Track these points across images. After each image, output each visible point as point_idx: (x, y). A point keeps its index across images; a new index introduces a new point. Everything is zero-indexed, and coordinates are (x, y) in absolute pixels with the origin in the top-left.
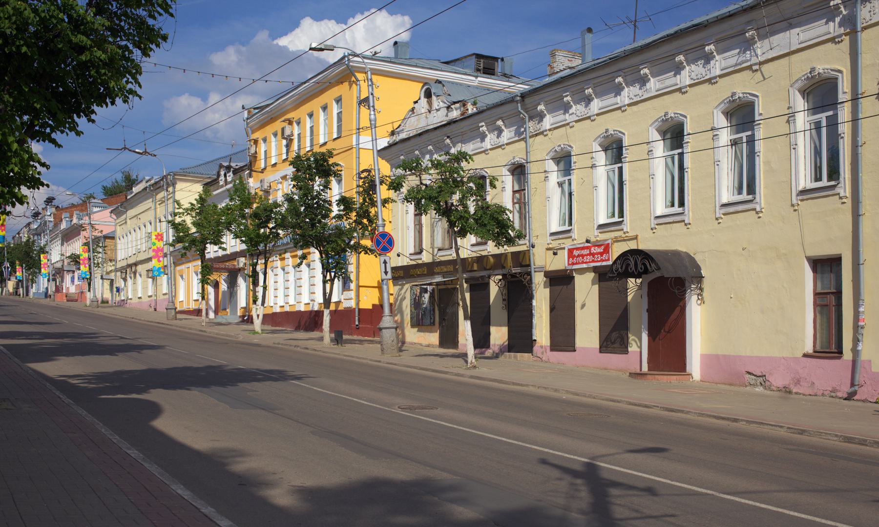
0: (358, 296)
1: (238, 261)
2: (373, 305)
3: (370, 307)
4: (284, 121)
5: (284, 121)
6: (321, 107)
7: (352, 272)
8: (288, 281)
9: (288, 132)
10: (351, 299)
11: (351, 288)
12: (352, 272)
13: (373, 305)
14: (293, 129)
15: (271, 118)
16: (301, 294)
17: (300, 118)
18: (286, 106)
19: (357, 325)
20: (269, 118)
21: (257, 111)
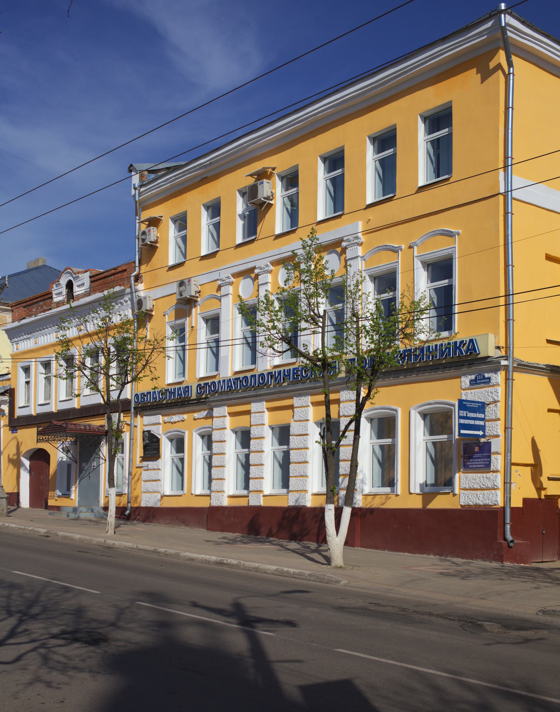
0: (507, 483)
2: (525, 501)
4: (251, 175)
6: (369, 137)
7: (498, 436)
8: (263, 451)
9: (265, 189)
10: (494, 488)
11: (492, 468)
12: (498, 436)
14: (274, 187)
15: (202, 179)
16: (307, 476)
17: (298, 165)
18: (250, 152)
19: (512, 541)
20: (199, 179)
21: (153, 176)
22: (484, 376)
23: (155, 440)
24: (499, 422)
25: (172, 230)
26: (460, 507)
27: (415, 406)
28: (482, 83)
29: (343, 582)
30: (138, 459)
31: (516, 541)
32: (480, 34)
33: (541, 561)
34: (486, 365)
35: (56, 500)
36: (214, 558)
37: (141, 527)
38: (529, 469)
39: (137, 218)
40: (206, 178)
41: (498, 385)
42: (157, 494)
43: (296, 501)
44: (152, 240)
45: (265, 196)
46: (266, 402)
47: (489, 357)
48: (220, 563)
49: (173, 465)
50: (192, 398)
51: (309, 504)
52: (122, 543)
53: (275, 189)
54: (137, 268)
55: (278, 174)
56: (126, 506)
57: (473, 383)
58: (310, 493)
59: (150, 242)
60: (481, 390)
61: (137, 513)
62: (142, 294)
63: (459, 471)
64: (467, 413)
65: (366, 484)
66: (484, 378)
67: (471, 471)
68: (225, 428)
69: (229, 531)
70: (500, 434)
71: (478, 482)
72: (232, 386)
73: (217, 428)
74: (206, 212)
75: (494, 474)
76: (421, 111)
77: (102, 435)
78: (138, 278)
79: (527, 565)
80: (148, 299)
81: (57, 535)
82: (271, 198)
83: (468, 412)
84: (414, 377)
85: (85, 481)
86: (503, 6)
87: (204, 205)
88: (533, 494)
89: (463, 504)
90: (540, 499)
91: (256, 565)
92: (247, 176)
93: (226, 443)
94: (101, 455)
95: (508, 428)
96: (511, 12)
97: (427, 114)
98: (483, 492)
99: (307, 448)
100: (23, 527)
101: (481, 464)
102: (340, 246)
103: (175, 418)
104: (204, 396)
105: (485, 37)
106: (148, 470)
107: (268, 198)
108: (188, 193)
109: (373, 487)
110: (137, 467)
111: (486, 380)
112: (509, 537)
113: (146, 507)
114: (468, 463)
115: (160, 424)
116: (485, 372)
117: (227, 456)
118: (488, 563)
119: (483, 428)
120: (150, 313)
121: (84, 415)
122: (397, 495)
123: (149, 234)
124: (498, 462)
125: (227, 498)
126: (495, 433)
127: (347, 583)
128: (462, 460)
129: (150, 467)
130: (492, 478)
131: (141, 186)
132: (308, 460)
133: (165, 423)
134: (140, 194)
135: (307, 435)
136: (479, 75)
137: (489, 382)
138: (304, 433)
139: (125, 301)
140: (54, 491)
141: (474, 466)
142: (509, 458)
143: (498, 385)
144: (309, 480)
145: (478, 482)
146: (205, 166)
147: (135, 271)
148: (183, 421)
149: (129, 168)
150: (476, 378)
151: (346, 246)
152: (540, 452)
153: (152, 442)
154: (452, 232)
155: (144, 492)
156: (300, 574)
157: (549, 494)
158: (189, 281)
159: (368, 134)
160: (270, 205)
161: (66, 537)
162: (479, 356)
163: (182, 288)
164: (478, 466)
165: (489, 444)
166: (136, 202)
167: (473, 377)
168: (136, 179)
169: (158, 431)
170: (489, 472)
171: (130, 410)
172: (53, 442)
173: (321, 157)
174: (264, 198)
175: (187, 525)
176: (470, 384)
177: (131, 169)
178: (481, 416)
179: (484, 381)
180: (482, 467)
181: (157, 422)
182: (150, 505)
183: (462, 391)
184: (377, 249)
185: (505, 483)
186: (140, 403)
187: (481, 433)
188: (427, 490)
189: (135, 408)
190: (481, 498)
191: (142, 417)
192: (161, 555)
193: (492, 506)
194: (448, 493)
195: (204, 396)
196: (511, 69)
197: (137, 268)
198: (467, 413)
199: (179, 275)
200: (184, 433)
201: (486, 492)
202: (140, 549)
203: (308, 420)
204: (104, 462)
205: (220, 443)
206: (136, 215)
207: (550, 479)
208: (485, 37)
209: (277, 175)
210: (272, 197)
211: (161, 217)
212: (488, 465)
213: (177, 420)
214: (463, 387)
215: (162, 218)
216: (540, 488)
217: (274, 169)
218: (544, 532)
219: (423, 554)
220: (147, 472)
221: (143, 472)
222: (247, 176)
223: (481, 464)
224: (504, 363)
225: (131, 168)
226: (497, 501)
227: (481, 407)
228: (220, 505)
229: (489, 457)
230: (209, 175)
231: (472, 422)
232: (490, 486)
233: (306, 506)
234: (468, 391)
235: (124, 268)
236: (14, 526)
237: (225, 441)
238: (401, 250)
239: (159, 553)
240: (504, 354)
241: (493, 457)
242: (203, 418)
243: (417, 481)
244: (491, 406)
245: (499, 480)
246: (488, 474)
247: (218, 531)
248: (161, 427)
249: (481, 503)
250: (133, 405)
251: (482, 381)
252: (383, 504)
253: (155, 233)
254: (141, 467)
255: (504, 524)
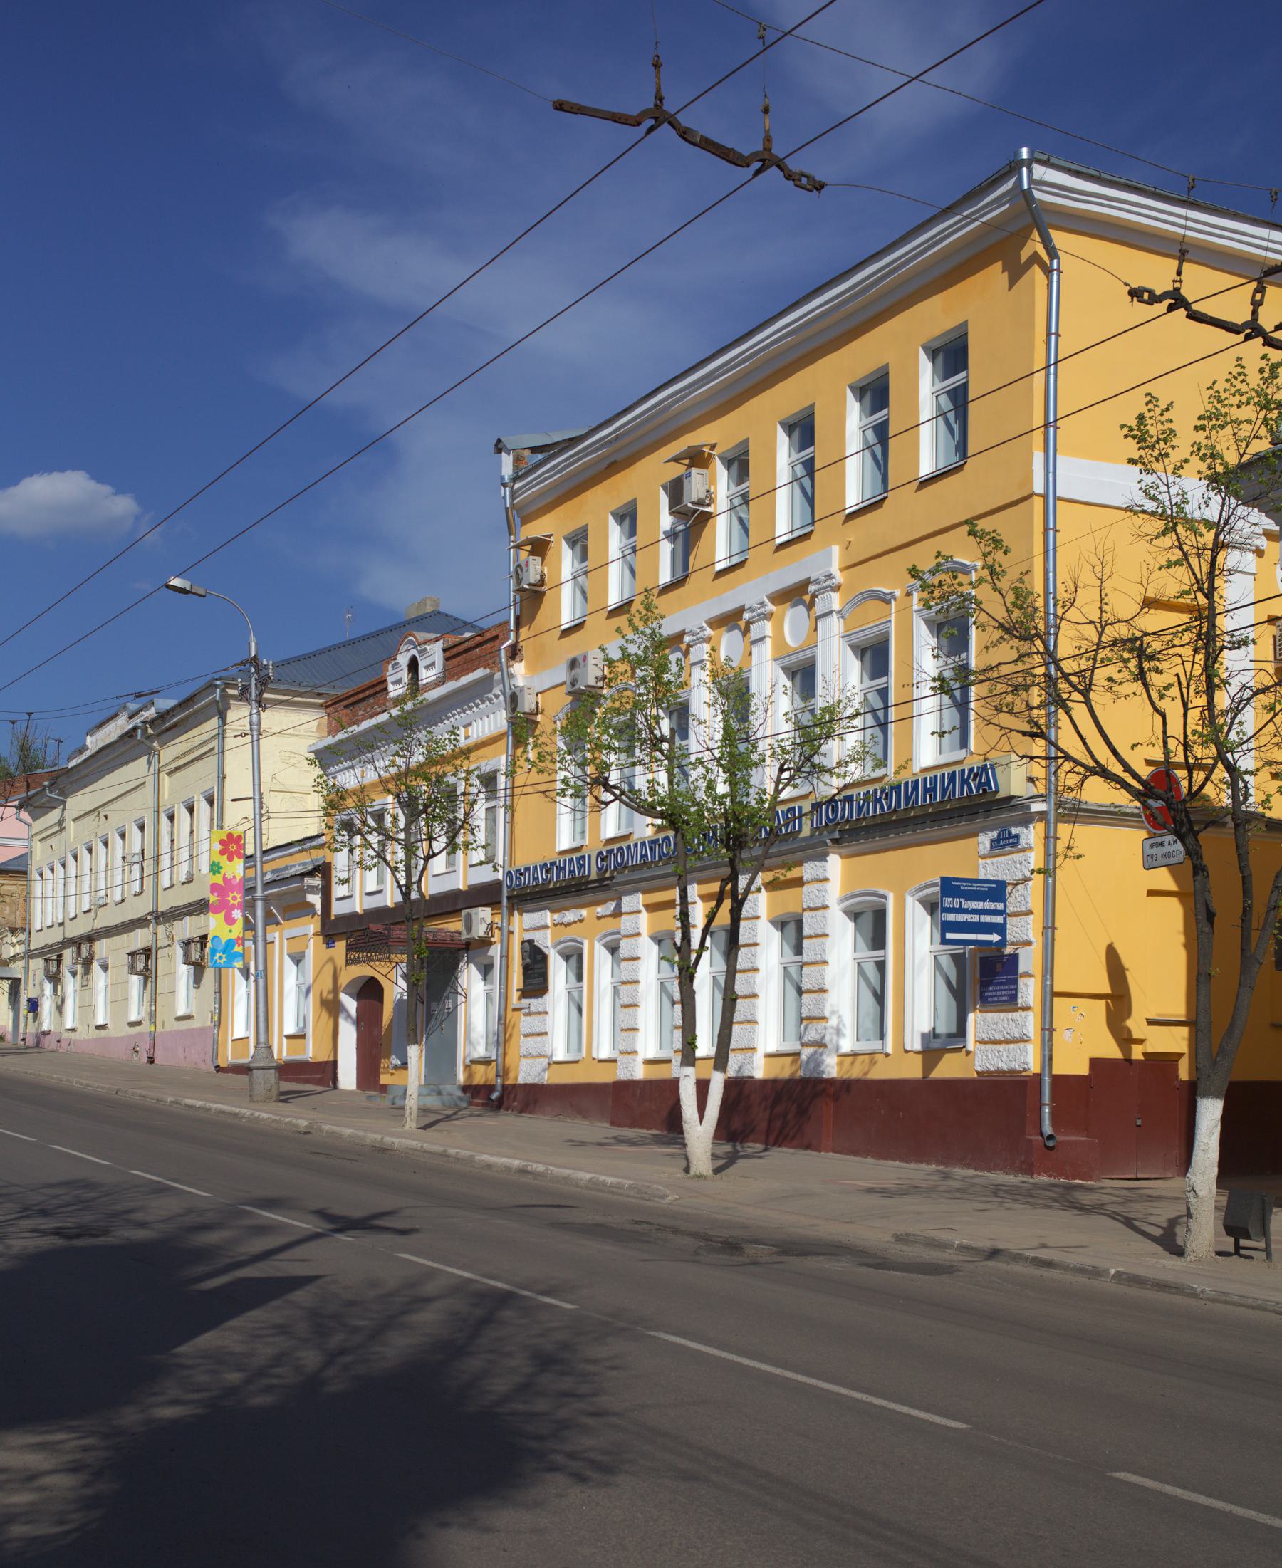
0: (1047, 1029)
1: (469, 917)
2: (1094, 1063)
3: (1084, 1070)
4: (676, 459)
5: (676, 459)
6: (851, 388)
7: (1029, 943)
9: (696, 487)
10: (1024, 1040)
11: (1020, 1002)
12: (1029, 943)
13: (1094, 1063)
14: (713, 480)
16: (755, 1022)
17: (747, 441)
19: (1050, 1137)
20: (605, 465)
21: (540, 457)
22: (1010, 833)
23: (539, 957)
24: (1031, 917)
25: (567, 561)
26: (976, 1075)
27: (912, 889)
28: (1010, 288)
29: (670, 1198)
30: (515, 995)
31: (1059, 1138)
32: (998, 202)
33: (1133, 1176)
34: (1010, 811)
35: (392, 1074)
36: (516, 1163)
37: (506, 1120)
38: (1101, 1004)
39: (512, 538)
40: (615, 462)
41: (1030, 848)
42: (542, 1059)
43: (740, 1068)
44: (532, 581)
45: (694, 498)
46: (699, 883)
47: (1013, 797)
48: (522, 1171)
49: (572, 1005)
50: (591, 879)
51: (759, 1074)
52: (404, 1141)
53: (715, 484)
54: (512, 635)
55: (724, 455)
56: (493, 1083)
57: (996, 844)
58: (761, 1052)
59: (529, 585)
60: (1007, 857)
61: (512, 1096)
62: (520, 682)
63: (974, 1009)
64: (961, 903)
65: (844, 1035)
66: (1010, 836)
67: (992, 1008)
68: (638, 934)
69: (642, 1127)
70: (1032, 939)
71: (1001, 1028)
72: (646, 855)
73: (627, 933)
74: (618, 527)
75: (1024, 1014)
76: (924, 340)
77: (459, 950)
78: (514, 653)
79: (1089, 1183)
80: (526, 692)
81: (321, 1131)
82: (707, 502)
83: (963, 900)
84: (909, 835)
85: (434, 1037)
86: (1025, 153)
87: (613, 514)
88: (1111, 1050)
89: (979, 1069)
90: (1128, 1060)
91: (566, 1172)
92: (668, 461)
93: (640, 961)
94: (459, 990)
95: (1049, 929)
96: (1049, 159)
97: (936, 345)
98: (1007, 1046)
99: (756, 970)
100: (278, 1118)
101: (1004, 995)
102: (806, 593)
103: (570, 916)
104: (608, 875)
105: (1007, 206)
106: (529, 1014)
107: (700, 503)
108: (589, 492)
109: (858, 1040)
110: (515, 1010)
111: (1013, 840)
112: (1047, 1129)
113: (525, 1085)
114: (987, 994)
115: (546, 927)
116: (1011, 826)
117: (642, 987)
118: (1012, 1177)
119: (1001, 929)
120: (532, 717)
121: (433, 913)
122: (887, 1055)
123: (527, 571)
124: (1030, 990)
125: (642, 1066)
126: (1025, 938)
127: (676, 1200)
128: (978, 987)
129: (533, 1009)
130: (1020, 1019)
131: (515, 479)
132: (757, 991)
133: (555, 925)
134: (514, 494)
135: (756, 944)
136: (1006, 274)
137: (1017, 843)
138: (751, 941)
139: (494, 695)
140: (389, 1058)
141: (995, 999)
142: (1048, 983)
143: (1030, 848)
144: (760, 1028)
145: (1001, 1028)
146: (610, 442)
147: (508, 638)
148: (581, 921)
149: (496, 445)
150: (999, 835)
151: (815, 591)
152: (1127, 973)
153: (535, 961)
154: (966, 566)
155: (525, 1057)
156: (620, 1186)
157: (1150, 1050)
158: (585, 658)
159: (850, 382)
160: (708, 516)
161: (331, 1134)
162: (999, 796)
163: (577, 671)
164: (1001, 999)
165: (1014, 958)
166: (507, 509)
167: (995, 834)
168: (507, 465)
169: (545, 940)
170: (1016, 1010)
171: (500, 902)
172: (377, 963)
173: (782, 424)
174: (693, 503)
175: (585, 1117)
176: (992, 847)
177: (499, 448)
178: (1000, 906)
179: (1010, 841)
180: (1005, 1001)
181: (543, 923)
182: (530, 1081)
183: (980, 861)
184: (860, 598)
185: (1043, 1029)
186: (514, 890)
187: (995, 938)
188: (936, 1044)
189: (508, 898)
190: (1005, 1058)
191: (521, 915)
192: (451, 1159)
193: (1020, 1072)
194: (959, 1050)
195: (608, 875)
196: (1055, 261)
197: (512, 635)
198: (961, 903)
199: (572, 646)
200: (582, 944)
201: (1012, 1046)
202: (425, 1152)
203: (757, 918)
204: (464, 1000)
205: (631, 962)
206: (510, 534)
207: (1151, 1022)
208: (1007, 206)
209: (720, 457)
210: (710, 499)
211: (550, 536)
212: (1014, 998)
213: (572, 920)
214: (981, 853)
215: (552, 539)
216: (1125, 1040)
217: (713, 447)
218: (1139, 1122)
219: (921, 1162)
220: (528, 1018)
221: (523, 1018)
222: (668, 461)
223: (1004, 995)
224: (1037, 807)
225: (500, 446)
226: (1026, 1063)
227: (997, 891)
228: (630, 1078)
229: (1015, 982)
230: (618, 457)
231: (974, 918)
232: (1017, 1035)
233: (752, 1077)
234: (988, 861)
235: (495, 633)
236: (265, 1115)
237: (638, 958)
238: (895, 599)
239: (448, 1156)
240: (1042, 791)
241: (1021, 982)
242: (610, 915)
243: (916, 1028)
244: (1019, 887)
245: (1030, 1023)
246: (1015, 1014)
247: (625, 1126)
248: (549, 932)
249: (1005, 1068)
250: (505, 892)
251: (1007, 842)
252: (866, 1074)
253: (539, 567)
254: (520, 1009)
255: (1040, 1105)
